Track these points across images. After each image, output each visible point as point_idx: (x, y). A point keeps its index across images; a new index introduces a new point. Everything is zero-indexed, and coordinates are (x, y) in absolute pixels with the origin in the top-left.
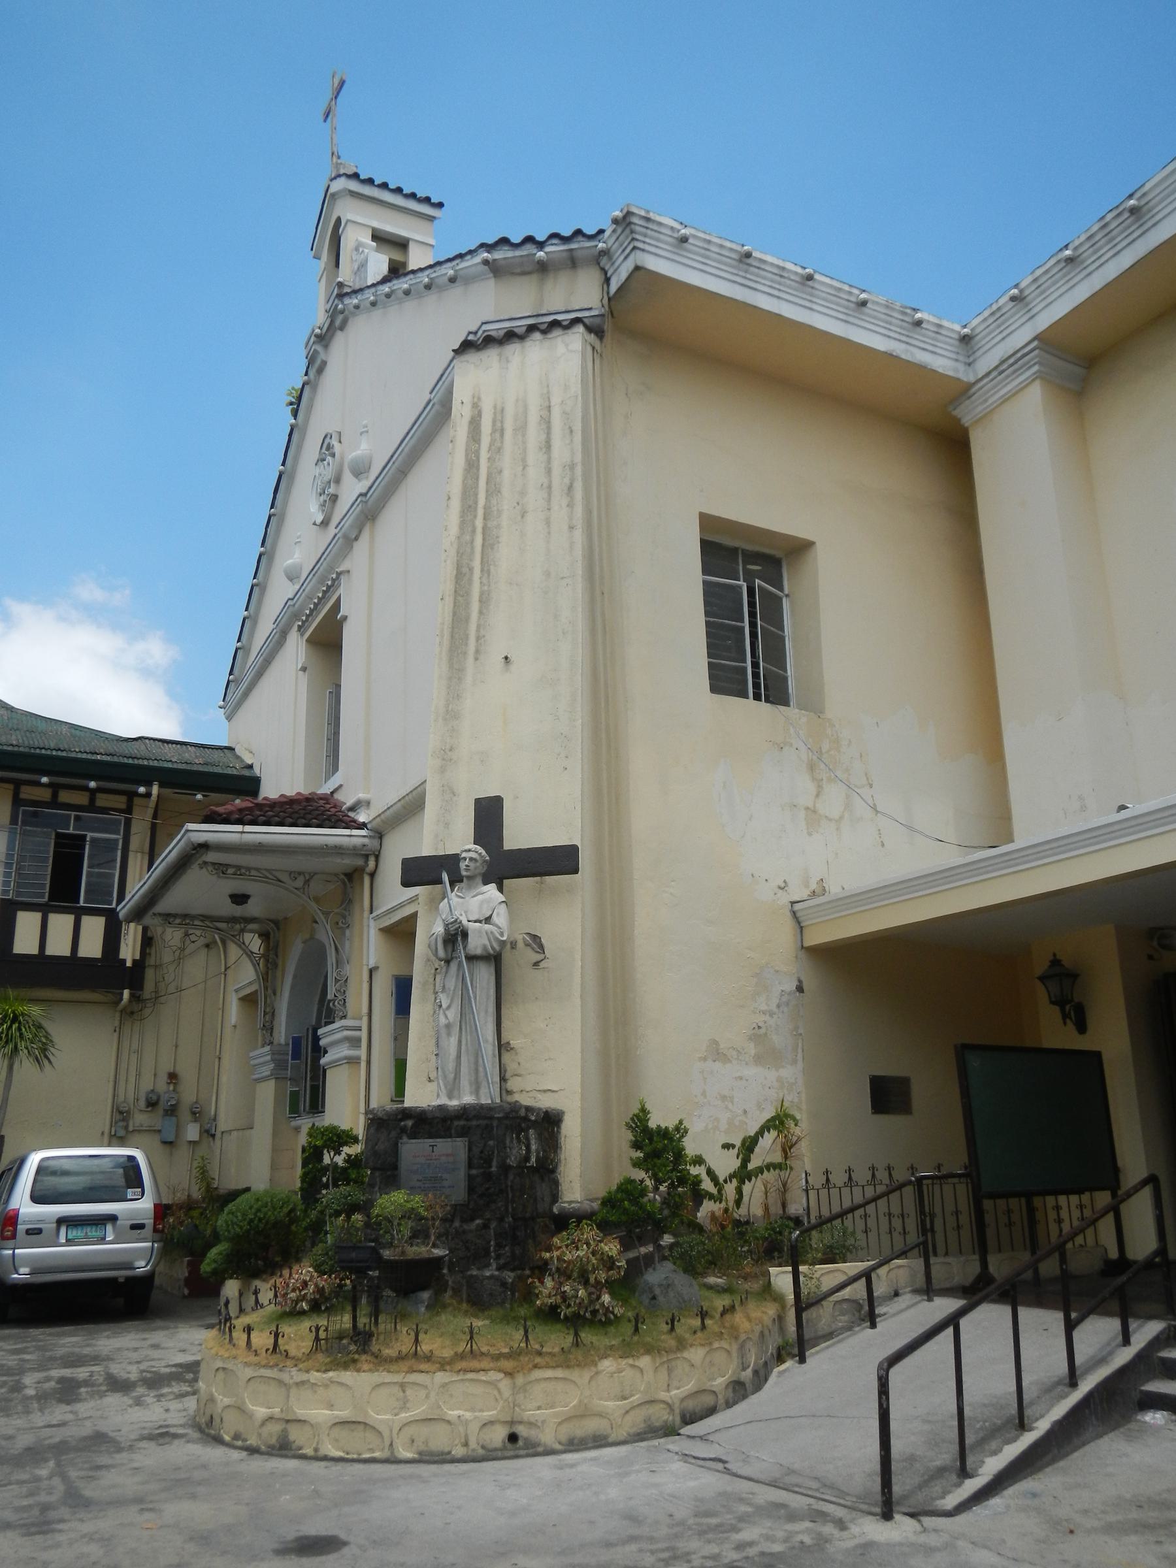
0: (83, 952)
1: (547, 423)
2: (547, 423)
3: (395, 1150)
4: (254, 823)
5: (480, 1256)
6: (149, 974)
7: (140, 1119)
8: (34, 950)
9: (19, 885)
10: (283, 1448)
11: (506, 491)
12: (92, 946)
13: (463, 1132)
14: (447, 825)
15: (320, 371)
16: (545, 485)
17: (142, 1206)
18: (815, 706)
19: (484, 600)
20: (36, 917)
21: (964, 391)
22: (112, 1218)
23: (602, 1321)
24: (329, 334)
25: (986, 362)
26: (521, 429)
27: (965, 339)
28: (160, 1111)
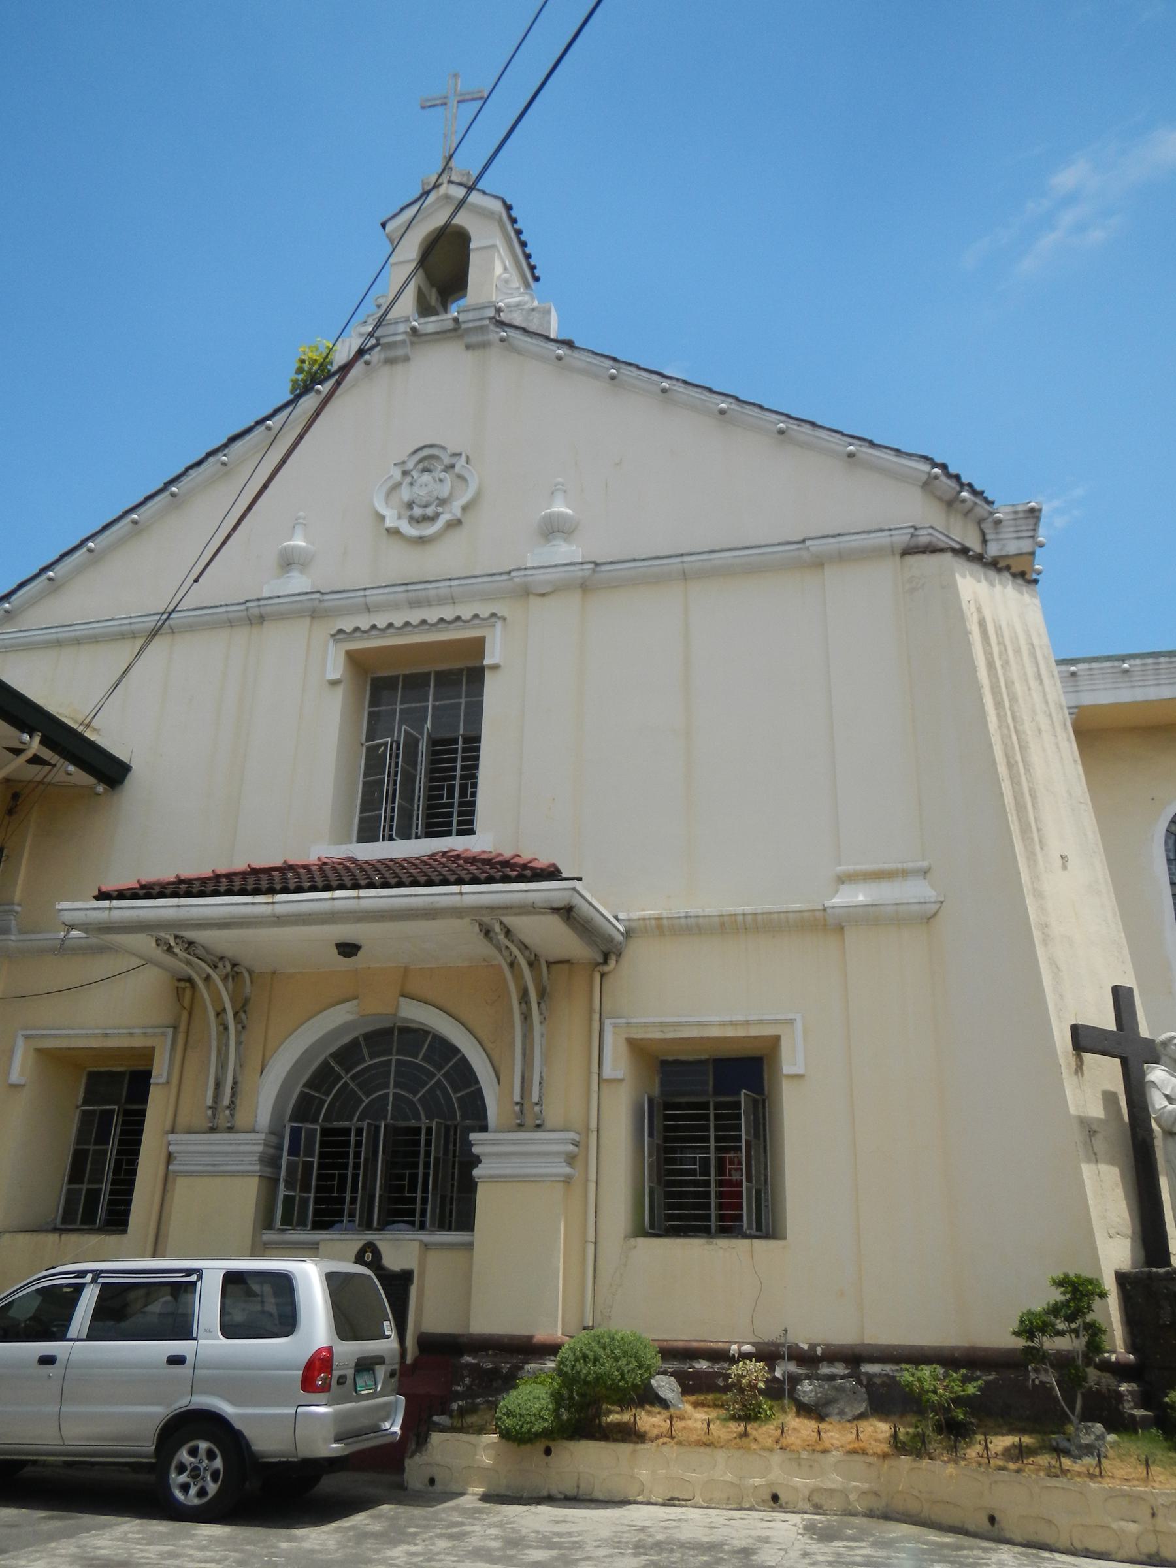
11: (1021, 701)
14: (1061, 996)
16: (1048, 713)
24: (429, 338)
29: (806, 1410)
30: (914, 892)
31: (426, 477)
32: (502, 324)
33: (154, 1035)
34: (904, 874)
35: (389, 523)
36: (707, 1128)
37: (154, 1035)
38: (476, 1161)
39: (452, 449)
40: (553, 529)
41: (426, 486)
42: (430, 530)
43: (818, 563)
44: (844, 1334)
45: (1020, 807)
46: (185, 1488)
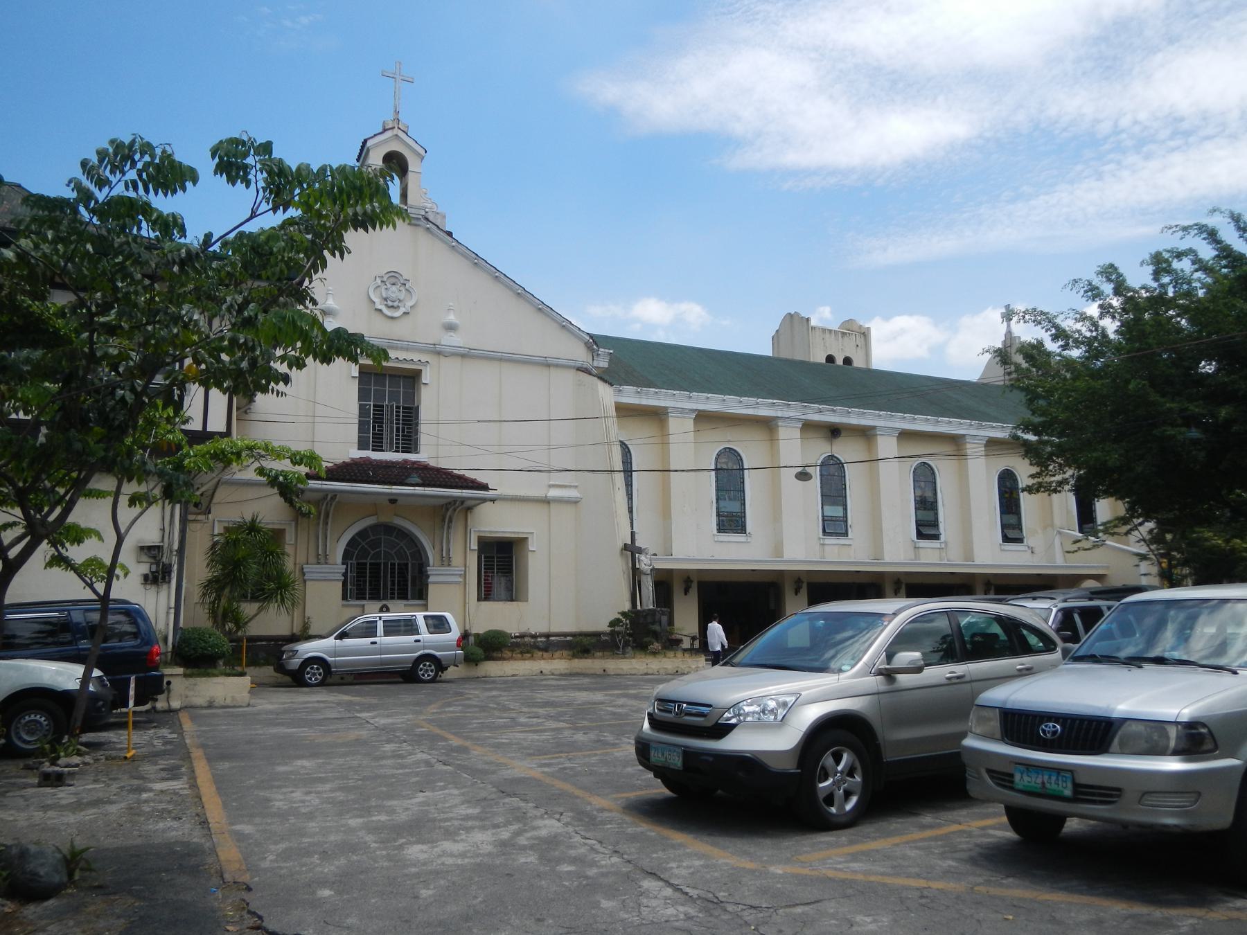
29: (539, 649)
30: (572, 494)
31: (394, 288)
32: (427, 219)
33: (285, 524)
34: (570, 487)
35: (379, 306)
36: (493, 565)
37: (285, 524)
38: (428, 577)
39: (405, 277)
40: (450, 328)
41: (394, 292)
42: (397, 314)
43: (549, 366)
44: (544, 630)
46: (429, 675)
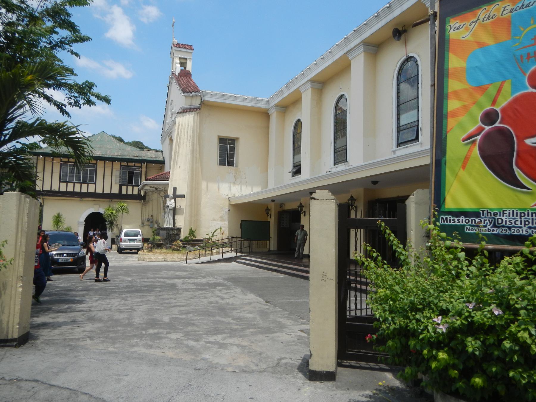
0: (134, 193)
1: (188, 128)
2: (188, 128)
3: (159, 232)
4: (154, 180)
5: (167, 244)
6: (147, 197)
7: (146, 223)
8: (125, 193)
9: (122, 181)
10: (144, 260)
12: (136, 192)
13: (166, 230)
15: (172, 83)
17: (140, 238)
18: (237, 166)
19: (178, 156)
20: (126, 187)
21: (268, 110)
22: (136, 239)
23: (178, 250)
25: (271, 106)
26: (184, 129)
27: (268, 101)
28: (150, 222)
45: (174, 159)
